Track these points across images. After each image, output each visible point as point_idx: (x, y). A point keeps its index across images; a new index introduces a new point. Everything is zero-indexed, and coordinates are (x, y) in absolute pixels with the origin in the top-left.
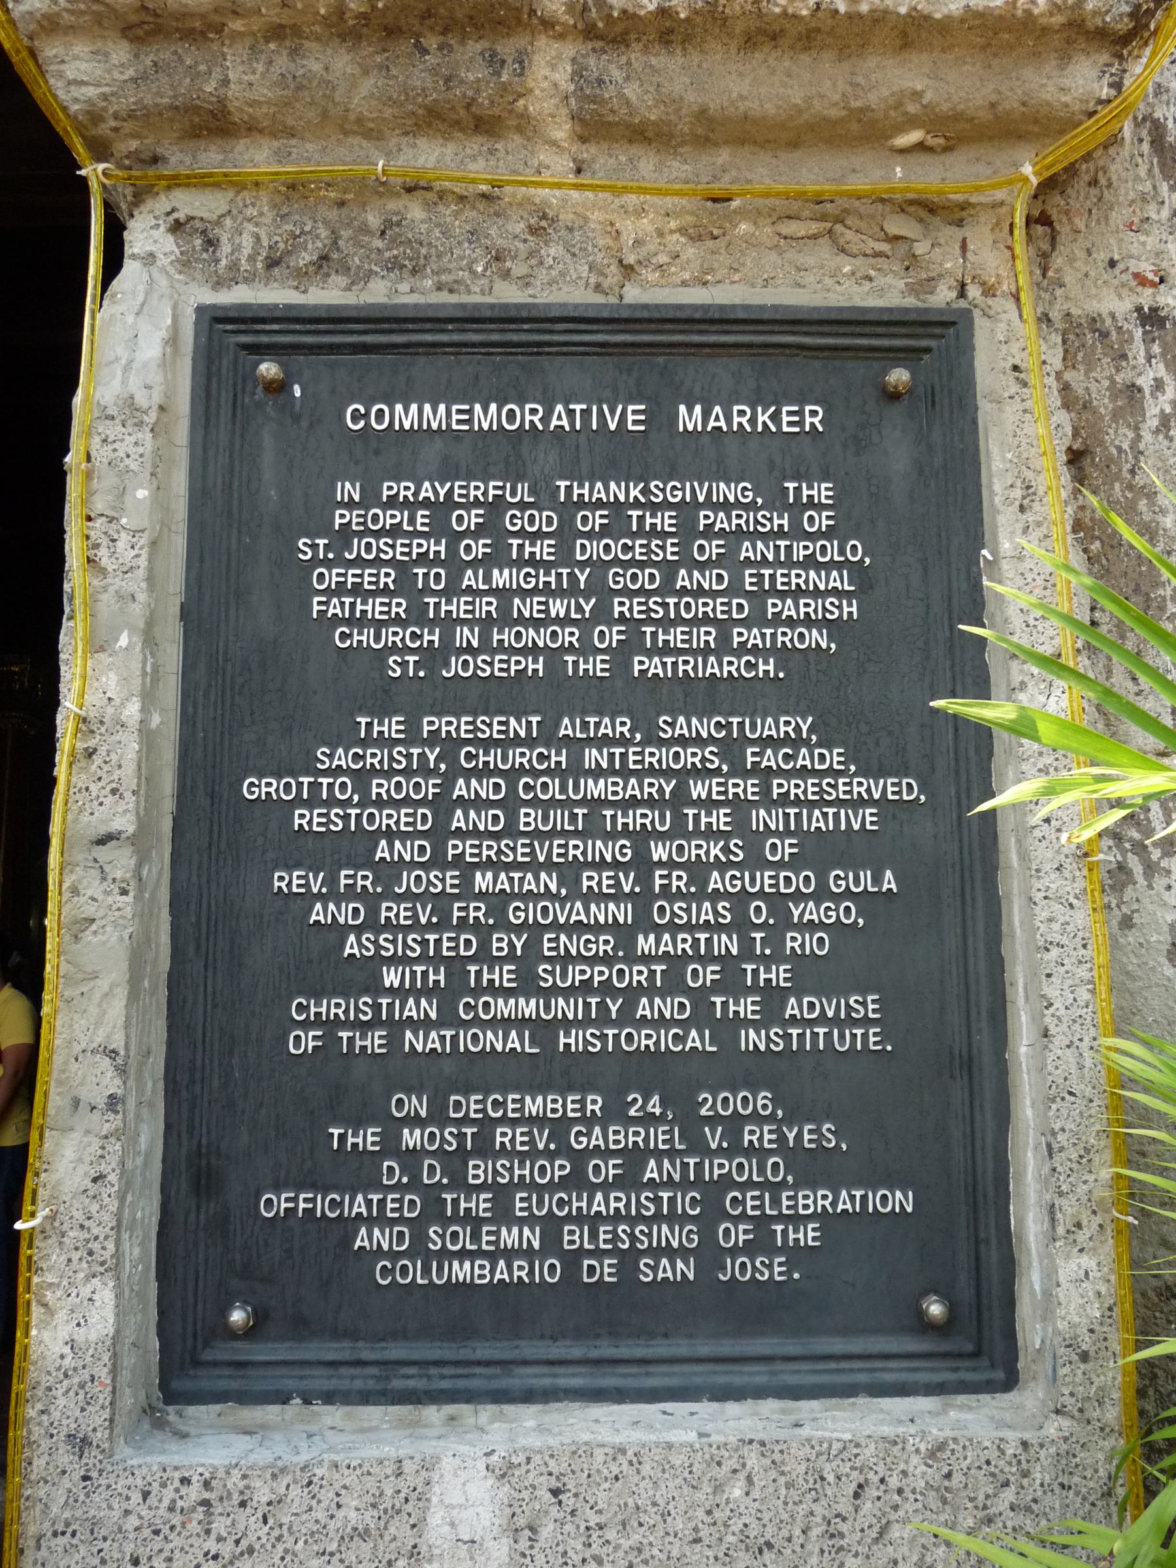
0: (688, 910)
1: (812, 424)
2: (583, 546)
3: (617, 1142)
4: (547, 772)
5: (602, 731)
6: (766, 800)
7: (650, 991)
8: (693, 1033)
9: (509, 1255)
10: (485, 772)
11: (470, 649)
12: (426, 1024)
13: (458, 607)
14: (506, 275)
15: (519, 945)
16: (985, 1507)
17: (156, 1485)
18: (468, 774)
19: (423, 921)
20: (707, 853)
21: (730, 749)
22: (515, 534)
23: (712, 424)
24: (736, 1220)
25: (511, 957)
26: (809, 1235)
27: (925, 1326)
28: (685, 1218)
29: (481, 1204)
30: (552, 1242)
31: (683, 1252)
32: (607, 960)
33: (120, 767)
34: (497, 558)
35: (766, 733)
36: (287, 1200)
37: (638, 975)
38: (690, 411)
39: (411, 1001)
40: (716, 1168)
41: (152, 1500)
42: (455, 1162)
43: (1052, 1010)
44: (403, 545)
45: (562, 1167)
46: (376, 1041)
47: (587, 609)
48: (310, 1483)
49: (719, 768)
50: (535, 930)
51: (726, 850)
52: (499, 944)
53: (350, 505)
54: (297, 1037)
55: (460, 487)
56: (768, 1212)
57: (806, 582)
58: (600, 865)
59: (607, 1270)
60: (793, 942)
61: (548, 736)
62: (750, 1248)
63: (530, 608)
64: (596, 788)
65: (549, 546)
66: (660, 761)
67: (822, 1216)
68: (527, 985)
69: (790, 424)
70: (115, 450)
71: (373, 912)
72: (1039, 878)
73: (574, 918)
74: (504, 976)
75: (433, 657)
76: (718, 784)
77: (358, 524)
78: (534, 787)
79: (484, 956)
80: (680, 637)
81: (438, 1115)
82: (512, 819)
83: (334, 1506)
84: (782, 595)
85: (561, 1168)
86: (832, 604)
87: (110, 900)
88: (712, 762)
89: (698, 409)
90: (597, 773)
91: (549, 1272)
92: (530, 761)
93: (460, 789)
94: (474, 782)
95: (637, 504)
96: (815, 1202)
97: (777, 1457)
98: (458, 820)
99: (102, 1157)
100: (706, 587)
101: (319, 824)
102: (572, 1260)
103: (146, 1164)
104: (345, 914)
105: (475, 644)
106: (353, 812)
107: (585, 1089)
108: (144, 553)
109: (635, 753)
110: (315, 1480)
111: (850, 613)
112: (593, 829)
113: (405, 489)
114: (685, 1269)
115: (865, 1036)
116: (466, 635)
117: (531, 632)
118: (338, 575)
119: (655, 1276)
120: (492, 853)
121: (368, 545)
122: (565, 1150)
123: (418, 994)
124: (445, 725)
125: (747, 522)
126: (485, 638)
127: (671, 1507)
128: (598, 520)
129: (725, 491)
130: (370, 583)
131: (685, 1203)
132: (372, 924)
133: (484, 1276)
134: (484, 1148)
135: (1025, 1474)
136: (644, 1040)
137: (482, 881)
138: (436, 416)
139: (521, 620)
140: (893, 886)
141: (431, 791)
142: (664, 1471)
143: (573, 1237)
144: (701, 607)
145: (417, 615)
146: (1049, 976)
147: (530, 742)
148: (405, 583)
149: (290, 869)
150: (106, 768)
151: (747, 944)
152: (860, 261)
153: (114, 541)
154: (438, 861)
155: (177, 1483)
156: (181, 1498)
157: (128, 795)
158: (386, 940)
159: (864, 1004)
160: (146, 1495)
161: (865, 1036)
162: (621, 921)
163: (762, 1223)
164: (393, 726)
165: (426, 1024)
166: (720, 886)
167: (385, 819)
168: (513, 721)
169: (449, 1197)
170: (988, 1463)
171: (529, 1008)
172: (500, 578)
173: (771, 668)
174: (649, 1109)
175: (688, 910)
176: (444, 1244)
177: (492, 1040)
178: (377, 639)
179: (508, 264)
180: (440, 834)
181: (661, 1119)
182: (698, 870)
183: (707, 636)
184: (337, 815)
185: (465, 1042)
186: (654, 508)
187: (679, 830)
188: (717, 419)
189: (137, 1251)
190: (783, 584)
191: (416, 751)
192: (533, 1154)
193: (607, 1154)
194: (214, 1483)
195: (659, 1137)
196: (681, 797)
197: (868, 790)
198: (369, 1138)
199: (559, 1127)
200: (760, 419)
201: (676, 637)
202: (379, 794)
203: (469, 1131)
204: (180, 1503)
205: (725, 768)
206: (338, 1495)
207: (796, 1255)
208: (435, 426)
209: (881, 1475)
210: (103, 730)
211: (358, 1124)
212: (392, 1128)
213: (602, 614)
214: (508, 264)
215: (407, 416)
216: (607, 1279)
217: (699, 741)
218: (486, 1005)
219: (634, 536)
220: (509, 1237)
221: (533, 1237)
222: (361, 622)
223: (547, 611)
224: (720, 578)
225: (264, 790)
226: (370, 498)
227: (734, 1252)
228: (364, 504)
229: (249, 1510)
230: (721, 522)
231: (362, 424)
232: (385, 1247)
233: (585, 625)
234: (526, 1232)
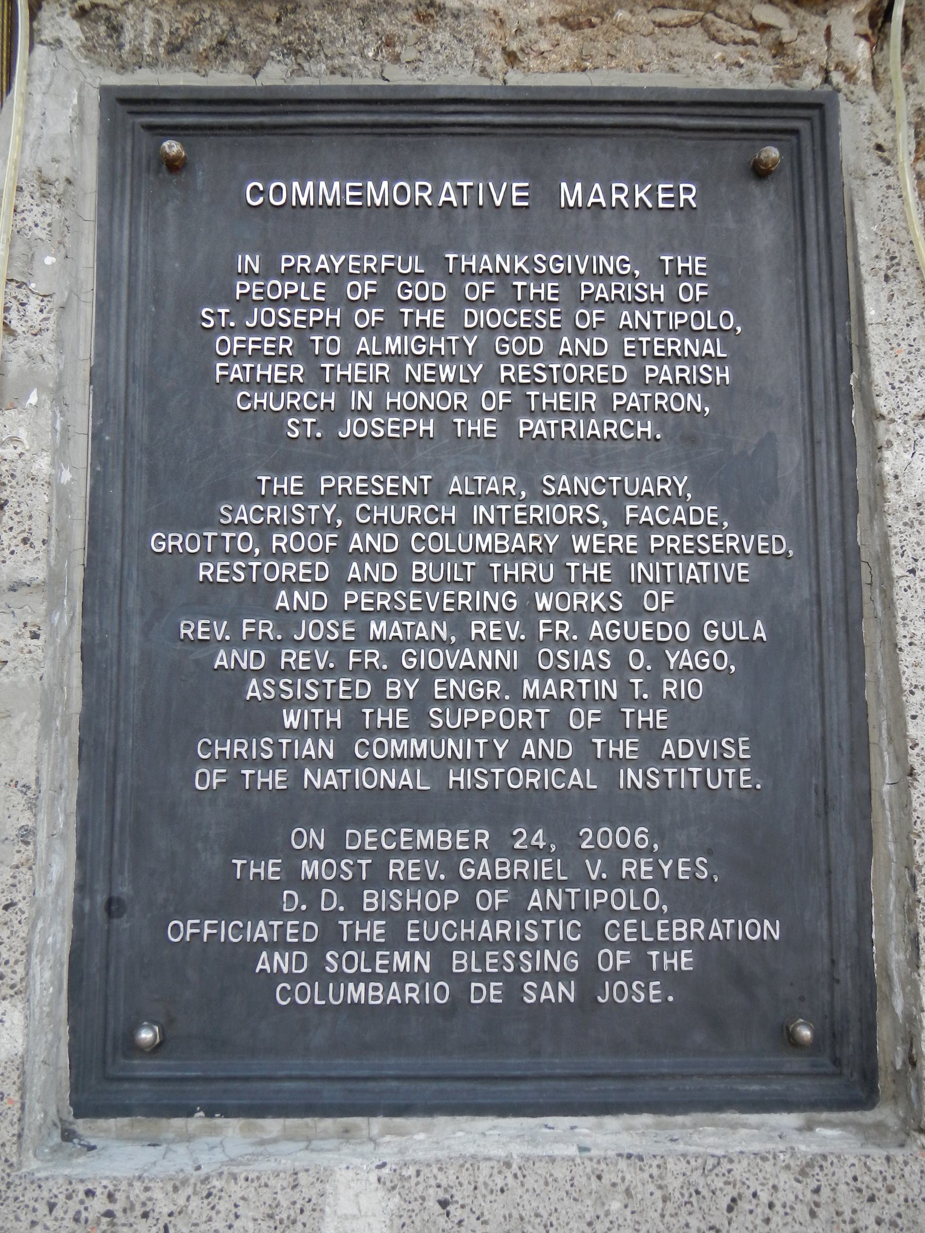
0: (571, 657)
1: (686, 200)
2: (471, 315)
3: (503, 873)
4: (439, 526)
5: (489, 488)
6: (646, 554)
7: (536, 733)
8: (576, 772)
9: (403, 977)
10: (381, 525)
11: (364, 411)
12: (323, 763)
13: (353, 371)
14: (397, 59)
15: (411, 689)
16: (852, 1221)
17: (62, 1197)
19: (321, 666)
20: (589, 602)
23: (592, 200)
24: (615, 946)
25: (405, 700)
26: (684, 961)
28: (567, 945)
29: (376, 930)
31: (565, 976)
32: (494, 702)
33: (30, 517)
35: (644, 491)
36: (193, 926)
37: (525, 717)
38: (571, 188)
39: (309, 741)
40: (597, 898)
41: (58, 1212)
43: (917, 750)
44: (300, 314)
45: (452, 896)
46: (277, 779)
47: (475, 374)
48: (209, 1195)
49: (600, 524)
50: (426, 675)
51: (606, 599)
52: (393, 688)
53: (251, 275)
54: (203, 775)
55: (355, 259)
56: (644, 939)
57: (682, 348)
58: (489, 613)
59: (492, 992)
61: (437, 492)
62: (627, 974)
64: (483, 542)
65: (439, 314)
66: (543, 517)
69: (665, 200)
70: (24, 219)
71: (274, 659)
72: (904, 625)
73: (463, 664)
74: (398, 717)
76: (599, 538)
77: (258, 294)
78: (426, 541)
80: (562, 400)
81: (336, 849)
82: (405, 570)
83: (232, 1217)
85: (450, 897)
86: (705, 369)
87: (21, 643)
88: (593, 518)
89: (578, 186)
90: (485, 527)
92: (421, 516)
93: (356, 542)
94: (369, 537)
95: (522, 275)
96: (689, 929)
97: (655, 1171)
98: (354, 572)
99: (14, 886)
100: (587, 352)
101: (223, 575)
103: (57, 893)
105: (369, 406)
106: (255, 564)
107: (473, 824)
108: (53, 317)
109: (520, 509)
110: (214, 1191)
111: (723, 379)
113: (301, 261)
114: (568, 992)
115: (737, 775)
117: (423, 396)
118: (240, 342)
119: (538, 998)
120: (386, 603)
121: (268, 314)
122: (454, 880)
123: (314, 733)
124: (342, 482)
125: (626, 292)
126: (379, 401)
127: (553, 1219)
128: (484, 289)
129: (607, 263)
130: (269, 349)
131: (569, 931)
132: (273, 669)
133: (377, 998)
135: (890, 1191)
136: (531, 778)
137: (377, 629)
139: (413, 384)
140: (763, 635)
141: (328, 544)
142: (547, 1184)
143: (461, 962)
145: (316, 377)
146: (914, 717)
147: (423, 498)
148: (304, 349)
149: (195, 617)
150: (16, 518)
151: (626, 689)
152: (731, 48)
153: (23, 304)
154: (335, 610)
155: (81, 1195)
156: (86, 1209)
157: (38, 544)
158: (286, 684)
160: (52, 1207)
161: (737, 775)
162: (508, 666)
163: (640, 948)
164: (292, 484)
165: (323, 763)
166: (600, 634)
167: (285, 570)
168: (405, 480)
169: (345, 924)
170: (855, 1179)
171: (420, 748)
172: (393, 344)
173: (649, 429)
174: (533, 843)
175: (571, 657)
176: (340, 965)
177: (385, 778)
178: (277, 400)
179: (398, 49)
181: (546, 851)
182: (581, 619)
183: (590, 399)
184: (239, 567)
185: (361, 779)
186: (539, 278)
187: (563, 581)
188: (597, 195)
189: (47, 974)
190: (660, 350)
191: (313, 507)
192: (425, 883)
193: (493, 884)
194: (118, 1195)
197: (741, 545)
198: (271, 869)
199: (450, 859)
200: (638, 196)
201: (559, 399)
202: (279, 547)
203: (364, 862)
204: (84, 1214)
205: (605, 523)
206: (236, 1206)
207: (672, 979)
208: (330, 202)
209: (752, 1190)
210: (14, 483)
211: (261, 854)
212: (292, 860)
214: (398, 49)
216: (493, 1000)
217: (580, 497)
219: (518, 304)
220: (402, 962)
222: (263, 385)
223: (438, 375)
224: (600, 344)
225: (171, 543)
226: (270, 269)
227: (614, 975)
228: (265, 274)
229: (151, 1221)
230: (600, 290)
231: (261, 200)
232: (285, 970)
234: (418, 956)
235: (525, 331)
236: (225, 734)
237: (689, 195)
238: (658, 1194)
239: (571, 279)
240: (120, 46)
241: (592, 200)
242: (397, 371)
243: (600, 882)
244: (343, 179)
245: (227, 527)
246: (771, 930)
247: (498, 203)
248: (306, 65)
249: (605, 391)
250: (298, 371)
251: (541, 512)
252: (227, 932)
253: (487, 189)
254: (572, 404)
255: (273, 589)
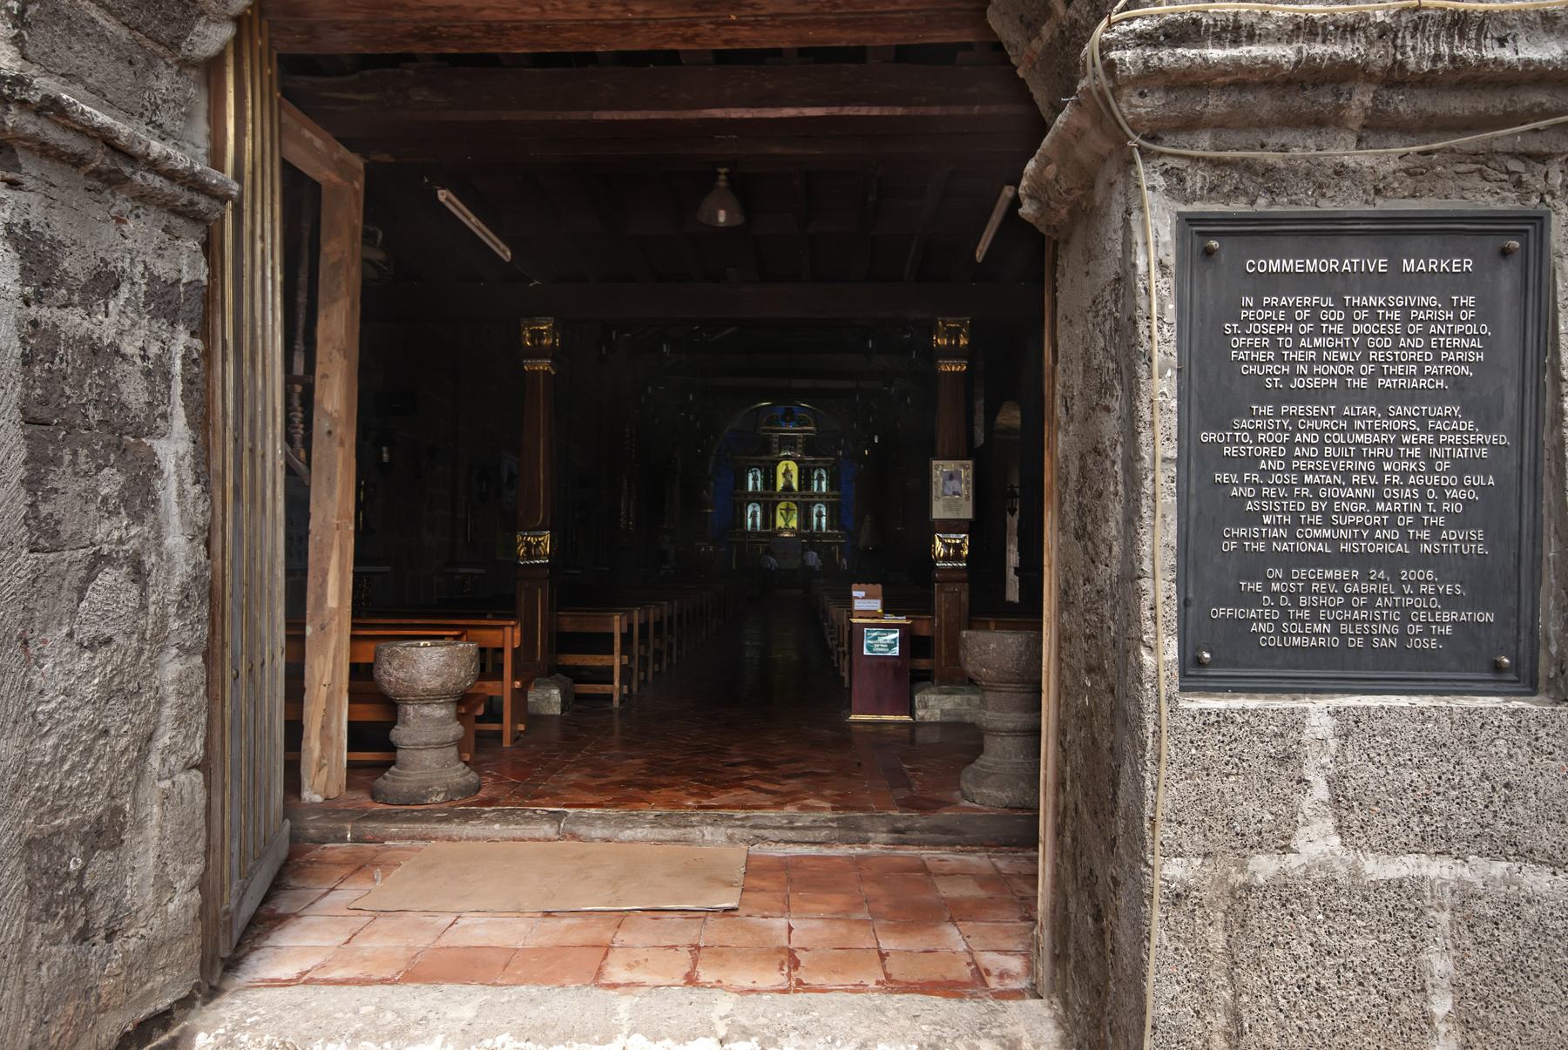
4: (1338, 431)
6: (1438, 445)
7: (1382, 527)
9: (1317, 635)
10: (1310, 430)
12: (1282, 539)
13: (1298, 355)
14: (1323, 195)
18: (1300, 431)
21: (1422, 421)
22: (1324, 322)
23: (1419, 268)
25: (1321, 512)
26: (1448, 630)
27: (1497, 668)
29: (1305, 614)
30: (1336, 630)
31: (1392, 636)
32: (1362, 513)
34: (1318, 333)
37: (1377, 520)
40: (1408, 601)
41: (1197, 720)
42: (1294, 597)
46: (1261, 546)
50: (1331, 500)
51: (1417, 466)
52: (1315, 506)
53: (1249, 308)
54: (1226, 545)
60: (1446, 506)
61: (1338, 415)
62: (1420, 635)
63: (1332, 356)
64: (1360, 438)
67: (1453, 623)
68: (1327, 523)
69: (1456, 268)
71: (1259, 492)
74: (1317, 519)
75: (1286, 378)
79: (1309, 511)
81: (1287, 577)
82: (1322, 451)
84: (1448, 350)
85: (1340, 600)
89: (1412, 261)
90: (1361, 431)
91: (1335, 642)
93: (1298, 438)
95: (1382, 307)
98: (1297, 452)
102: (1344, 638)
104: (1248, 492)
105: (1306, 372)
108: (1175, 333)
112: (1359, 456)
113: (1273, 300)
115: (1476, 548)
116: (1301, 368)
121: (1257, 327)
123: (1277, 526)
126: (1310, 369)
128: (1363, 314)
129: (1423, 300)
131: (1394, 615)
132: (1259, 496)
134: (1307, 591)
137: (1308, 479)
138: (1288, 265)
139: (1327, 362)
144: (1411, 355)
145: (1280, 359)
147: (1330, 417)
148: (1274, 345)
149: (1222, 472)
152: (1494, 185)
154: (1289, 470)
159: (1477, 534)
161: (1476, 548)
165: (1282, 539)
167: (1265, 451)
168: (1322, 408)
169: (1291, 611)
171: (1328, 533)
172: (1318, 342)
175: (1400, 493)
180: (1289, 457)
181: (1385, 580)
182: (1405, 474)
183: (1413, 369)
185: (1299, 546)
186: (1390, 309)
187: (1397, 456)
191: (1278, 421)
192: (1329, 594)
193: (1359, 595)
195: (1383, 588)
196: (1399, 442)
198: (1258, 586)
199: (1340, 583)
200: (1442, 266)
207: (1441, 638)
208: (1288, 270)
211: (1253, 579)
213: (1365, 359)
215: (1275, 266)
218: (1309, 532)
219: (1379, 322)
220: (1317, 628)
221: (1327, 628)
222: (1254, 362)
223: (1339, 358)
226: (1258, 304)
227: (1415, 636)
228: (1254, 308)
233: (1356, 363)
234: (1325, 626)
235: (1382, 336)
236: (1237, 526)
237: (1468, 264)
238: (1449, 721)
239: (1406, 310)
240: (1185, 190)
241: (1419, 268)
242: (1320, 355)
243: (1410, 595)
244: (1295, 258)
245: (1236, 430)
246: (1489, 617)
247: (1371, 270)
248: (1277, 199)
249: (1421, 365)
250: (1271, 355)
251: (1386, 424)
252: (1238, 613)
253: (1366, 263)
254: (1405, 372)
255: (1258, 459)
